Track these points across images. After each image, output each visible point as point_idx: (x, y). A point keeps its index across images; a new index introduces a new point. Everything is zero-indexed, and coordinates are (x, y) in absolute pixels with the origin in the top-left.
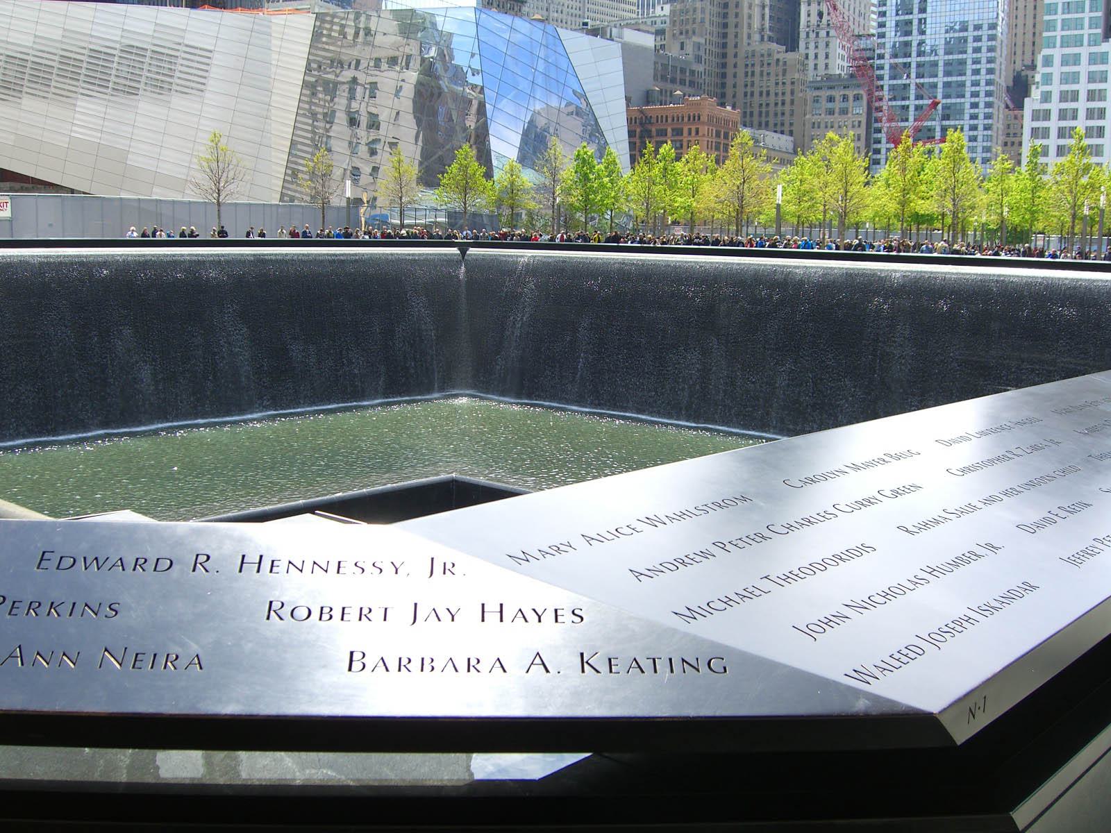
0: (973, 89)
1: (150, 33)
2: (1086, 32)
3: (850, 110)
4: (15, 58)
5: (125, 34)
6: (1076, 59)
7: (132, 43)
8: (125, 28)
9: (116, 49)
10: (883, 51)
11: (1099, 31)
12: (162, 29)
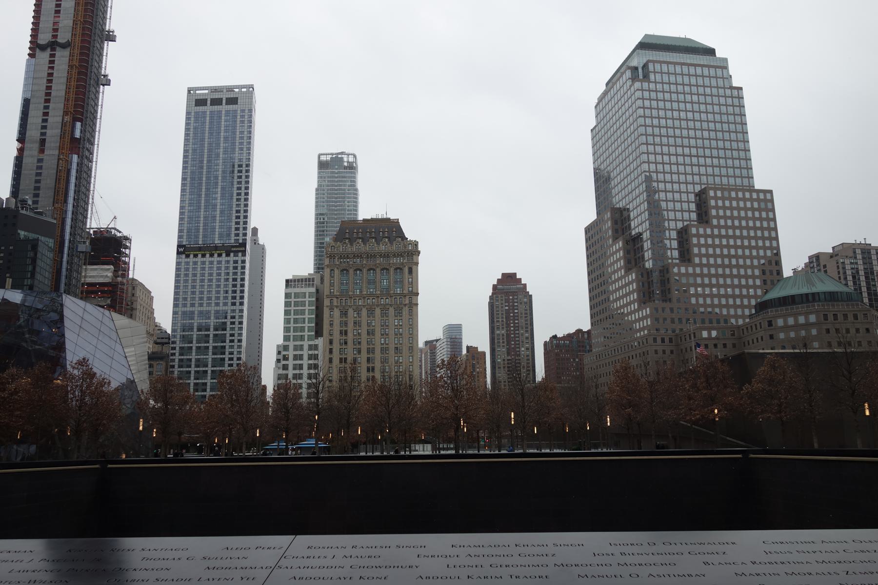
0: (230, 362)
2: (306, 333)
3: (154, 372)
6: (301, 348)
10: (175, 339)
11: (313, 333)
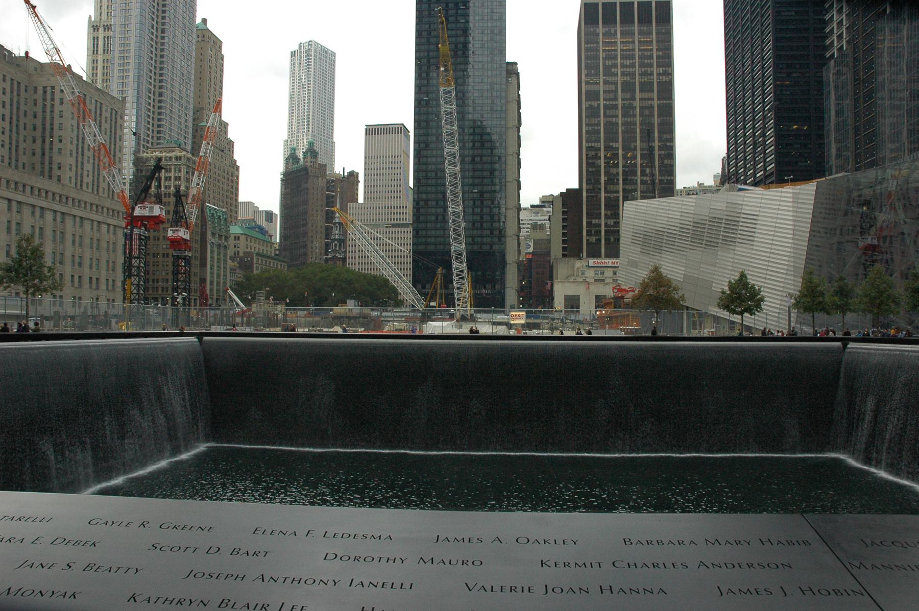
1: (724, 209)
4: (659, 231)
5: (711, 211)
7: (715, 216)
8: (711, 207)
9: (706, 220)
12: (731, 205)
